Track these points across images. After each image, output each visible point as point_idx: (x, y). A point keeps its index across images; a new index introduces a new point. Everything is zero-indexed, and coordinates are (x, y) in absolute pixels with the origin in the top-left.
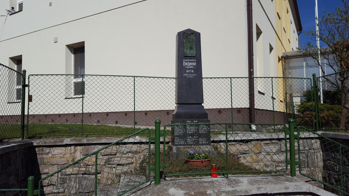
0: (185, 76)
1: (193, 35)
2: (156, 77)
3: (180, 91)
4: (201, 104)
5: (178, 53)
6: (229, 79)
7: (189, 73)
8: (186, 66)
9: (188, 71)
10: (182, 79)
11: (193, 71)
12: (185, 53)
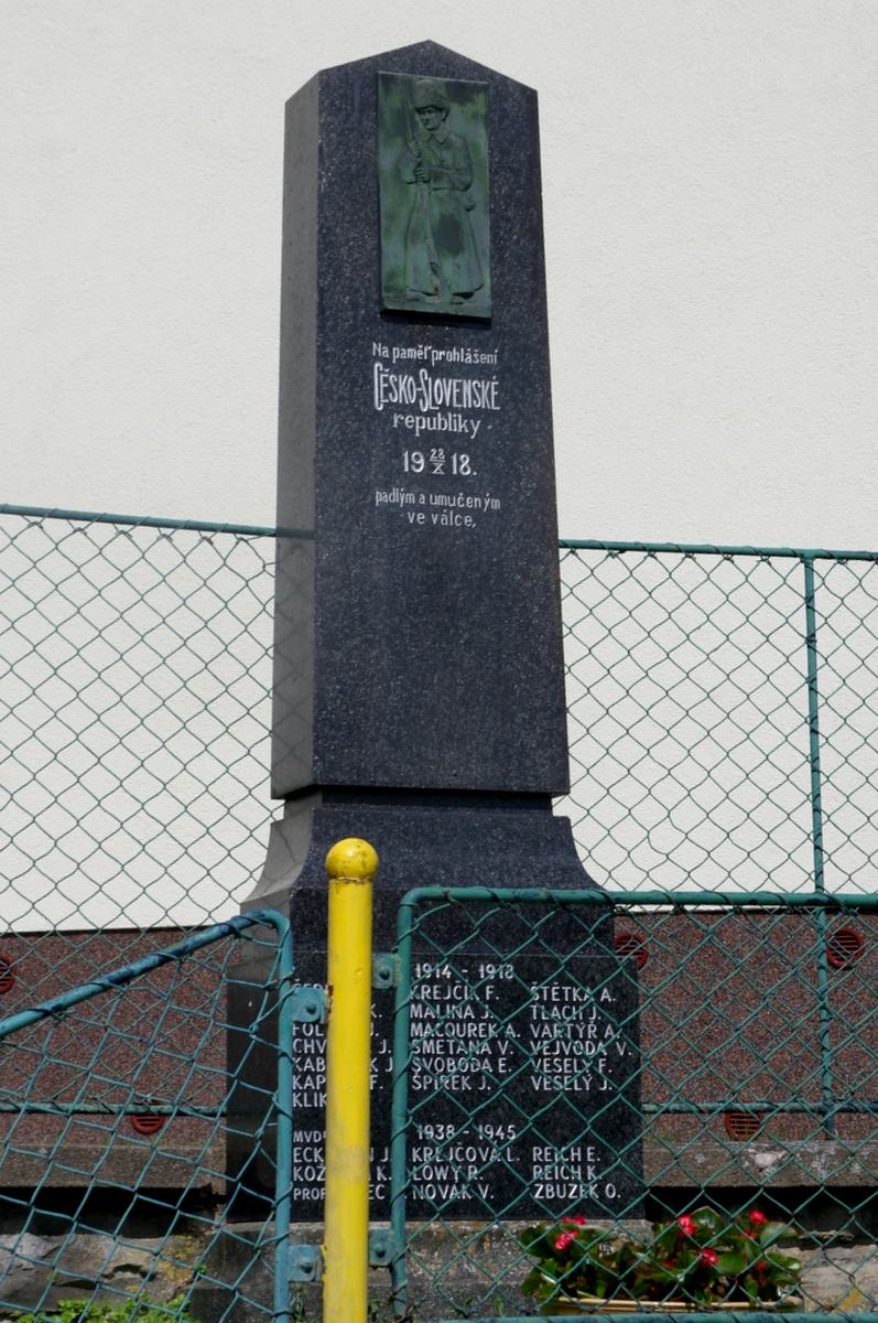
0: (392, 511)
1: (469, 108)
2: (55, 514)
3: (338, 656)
4: (542, 800)
5: (321, 275)
6: (793, 570)
7: (428, 482)
8: (404, 409)
9: (415, 463)
10: (364, 538)
11: (463, 465)
12: (392, 275)
